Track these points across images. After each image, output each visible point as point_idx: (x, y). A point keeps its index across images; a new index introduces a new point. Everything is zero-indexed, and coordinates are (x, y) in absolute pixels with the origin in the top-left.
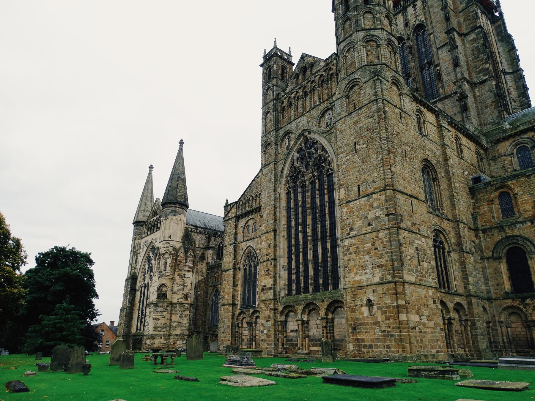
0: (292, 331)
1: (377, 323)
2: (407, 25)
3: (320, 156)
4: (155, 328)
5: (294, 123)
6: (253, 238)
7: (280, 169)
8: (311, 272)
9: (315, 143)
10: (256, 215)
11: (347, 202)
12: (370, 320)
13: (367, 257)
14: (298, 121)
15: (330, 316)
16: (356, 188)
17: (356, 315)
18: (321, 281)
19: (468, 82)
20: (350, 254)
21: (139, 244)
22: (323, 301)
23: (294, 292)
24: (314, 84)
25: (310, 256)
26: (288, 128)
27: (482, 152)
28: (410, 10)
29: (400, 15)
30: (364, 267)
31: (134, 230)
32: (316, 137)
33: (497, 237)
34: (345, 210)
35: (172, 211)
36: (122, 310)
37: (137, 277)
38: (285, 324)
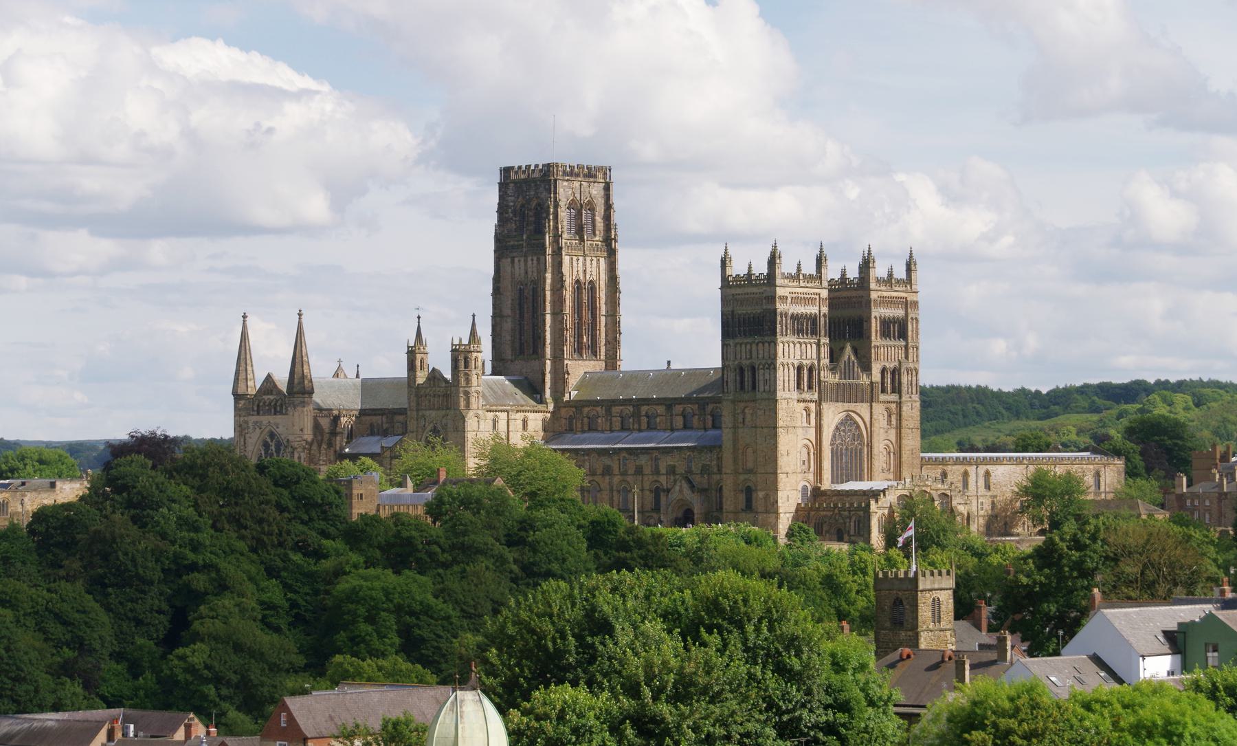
2: (526, 273)
21: (247, 422)
28: (529, 259)
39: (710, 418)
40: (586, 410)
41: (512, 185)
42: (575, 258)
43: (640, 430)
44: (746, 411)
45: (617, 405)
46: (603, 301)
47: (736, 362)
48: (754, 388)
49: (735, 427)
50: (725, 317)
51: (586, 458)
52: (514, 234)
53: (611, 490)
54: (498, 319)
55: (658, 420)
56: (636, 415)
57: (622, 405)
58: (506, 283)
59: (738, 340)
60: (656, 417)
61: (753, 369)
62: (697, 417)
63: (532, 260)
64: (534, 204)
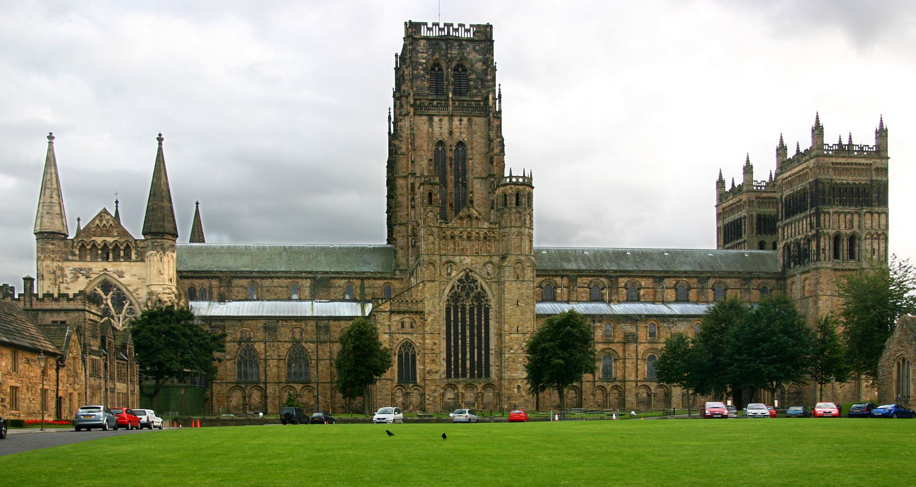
0: (449, 399)
1: (522, 396)
2: (451, 133)
3: (479, 293)
5: (457, 258)
6: (412, 334)
7: (443, 288)
8: (468, 365)
9: (475, 281)
10: (414, 316)
11: (510, 333)
12: (518, 394)
13: (519, 365)
14: (462, 258)
15: (483, 391)
16: (516, 328)
17: (511, 392)
18: (476, 372)
20: (509, 362)
22: (480, 383)
23: (453, 376)
24: (477, 235)
25: (468, 356)
26: (451, 258)
30: (517, 370)
32: (477, 277)
34: (507, 337)
38: (443, 395)
41: (422, 42)
43: (619, 302)
45: (587, 276)
47: (832, 232)
48: (852, 256)
52: (427, 92)
55: (642, 292)
56: (613, 287)
57: (591, 276)
59: (836, 209)
60: (639, 289)
61: (852, 239)
62: (693, 290)
63: (461, 120)
64: (454, 64)
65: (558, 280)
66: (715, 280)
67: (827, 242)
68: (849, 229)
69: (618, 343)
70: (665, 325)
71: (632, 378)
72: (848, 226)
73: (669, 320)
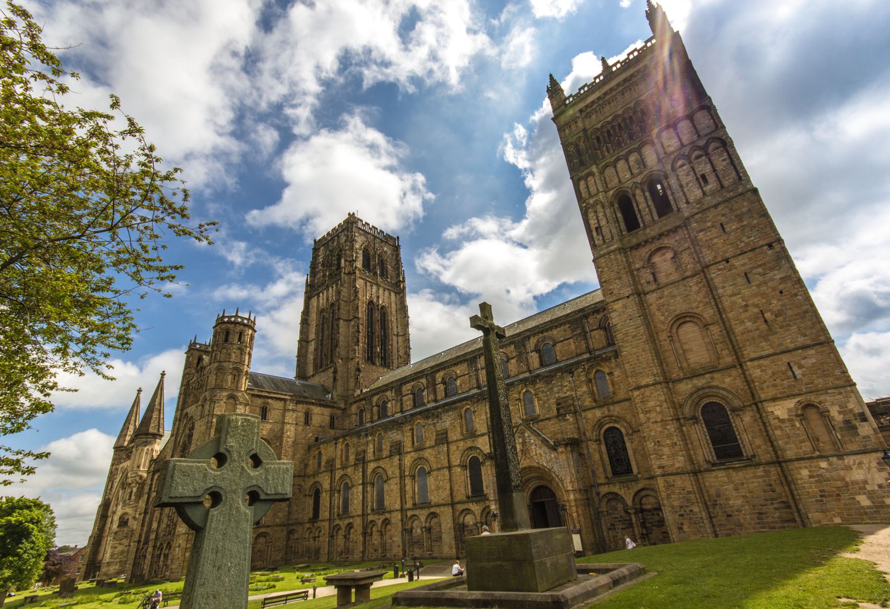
2: (328, 299)
4: (112, 556)
19: (342, 359)
21: (117, 469)
27: (339, 412)
28: (330, 289)
29: (325, 292)
31: (115, 454)
33: (312, 481)
35: (144, 442)
36: (90, 537)
37: (110, 503)
39: (535, 355)
40: (375, 399)
42: (368, 284)
44: (656, 259)
46: (395, 324)
49: (640, 294)
50: (571, 149)
51: (370, 438)
53: (402, 477)
54: (304, 344)
55: (458, 382)
57: (413, 380)
58: (313, 316)
60: (455, 380)
62: (513, 361)
65: (388, 393)
66: (537, 337)
67: (601, 215)
68: (640, 174)
69: (386, 458)
70: (430, 421)
71: (398, 506)
72: (636, 171)
73: (433, 414)
